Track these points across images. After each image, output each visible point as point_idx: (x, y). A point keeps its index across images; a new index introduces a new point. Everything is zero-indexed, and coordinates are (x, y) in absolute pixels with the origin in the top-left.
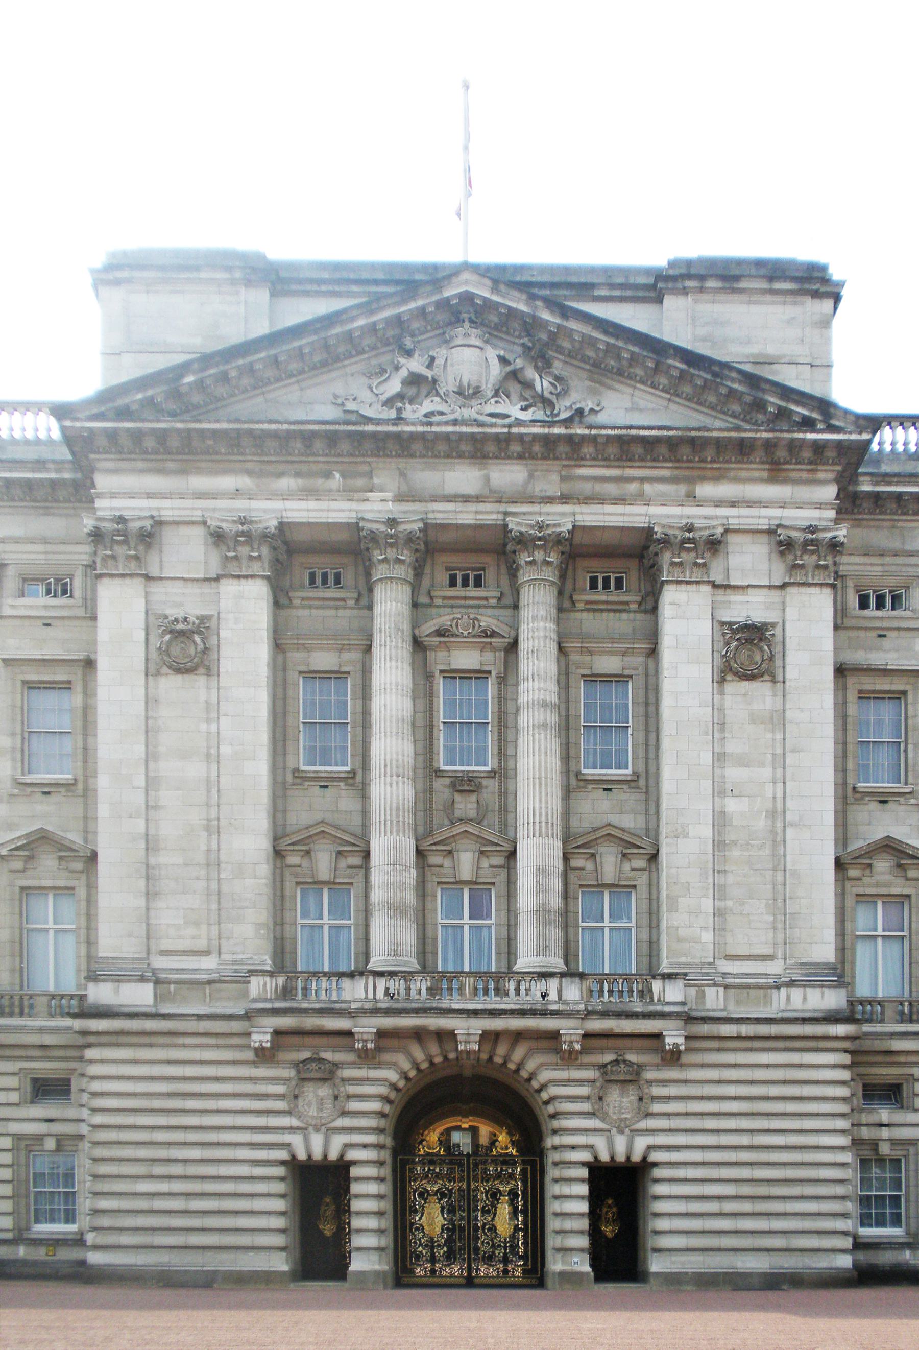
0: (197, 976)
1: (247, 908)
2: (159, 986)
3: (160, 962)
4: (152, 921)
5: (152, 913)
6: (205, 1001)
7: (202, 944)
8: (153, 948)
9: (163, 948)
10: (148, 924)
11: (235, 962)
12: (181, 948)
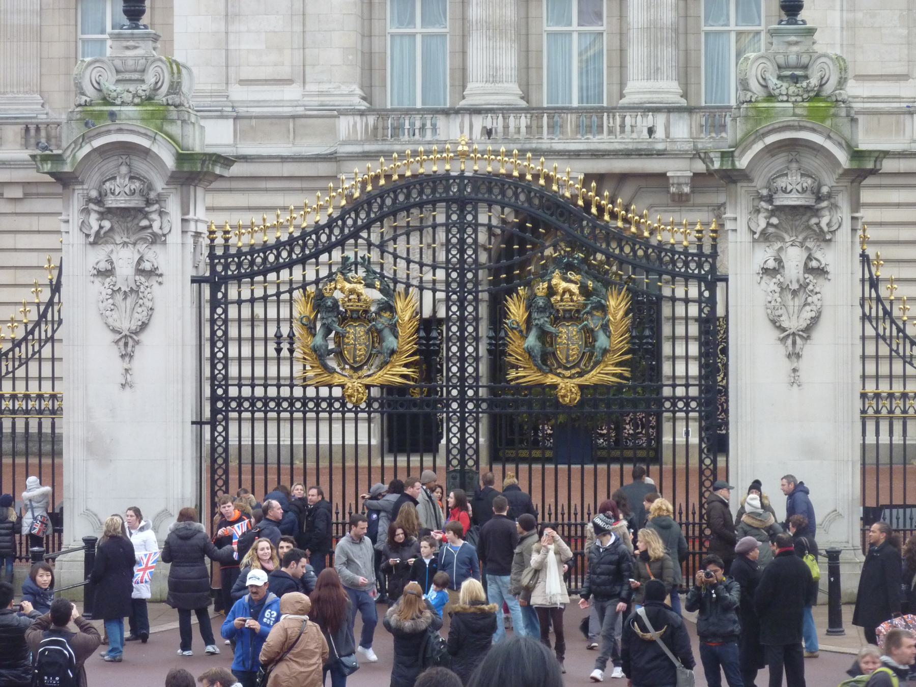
0: (280, 109)
1: (334, 30)
2: (238, 121)
3: (238, 93)
4: (232, 47)
5: (232, 38)
6: (288, 137)
7: (285, 72)
8: (232, 76)
9: (244, 76)
10: (227, 50)
11: (321, 94)
12: (262, 76)
